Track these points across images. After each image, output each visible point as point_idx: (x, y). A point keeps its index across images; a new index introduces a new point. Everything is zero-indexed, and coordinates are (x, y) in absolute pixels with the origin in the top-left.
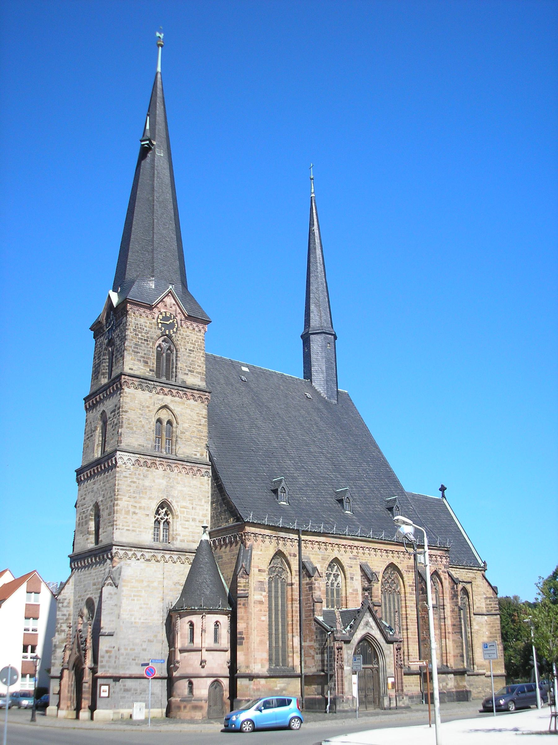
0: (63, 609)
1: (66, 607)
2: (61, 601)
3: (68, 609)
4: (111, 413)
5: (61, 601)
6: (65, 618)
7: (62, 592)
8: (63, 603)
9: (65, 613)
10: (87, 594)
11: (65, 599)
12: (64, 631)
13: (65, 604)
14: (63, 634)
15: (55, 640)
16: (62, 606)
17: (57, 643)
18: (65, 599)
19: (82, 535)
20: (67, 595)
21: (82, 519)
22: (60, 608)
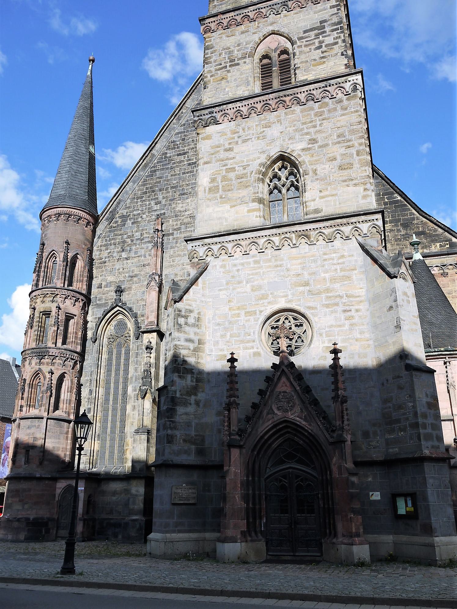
0: (187, 329)
1: (194, 325)
2: (183, 313)
3: (196, 329)
4: (305, 32)
5: (183, 313)
6: (191, 346)
7: (185, 298)
8: (186, 317)
9: (192, 336)
10: (276, 302)
11: (191, 311)
13: (191, 320)
14: (189, 377)
16: (186, 324)
17: (178, 395)
18: (191, 311)
19: (227, 207)
21: (224, 178)
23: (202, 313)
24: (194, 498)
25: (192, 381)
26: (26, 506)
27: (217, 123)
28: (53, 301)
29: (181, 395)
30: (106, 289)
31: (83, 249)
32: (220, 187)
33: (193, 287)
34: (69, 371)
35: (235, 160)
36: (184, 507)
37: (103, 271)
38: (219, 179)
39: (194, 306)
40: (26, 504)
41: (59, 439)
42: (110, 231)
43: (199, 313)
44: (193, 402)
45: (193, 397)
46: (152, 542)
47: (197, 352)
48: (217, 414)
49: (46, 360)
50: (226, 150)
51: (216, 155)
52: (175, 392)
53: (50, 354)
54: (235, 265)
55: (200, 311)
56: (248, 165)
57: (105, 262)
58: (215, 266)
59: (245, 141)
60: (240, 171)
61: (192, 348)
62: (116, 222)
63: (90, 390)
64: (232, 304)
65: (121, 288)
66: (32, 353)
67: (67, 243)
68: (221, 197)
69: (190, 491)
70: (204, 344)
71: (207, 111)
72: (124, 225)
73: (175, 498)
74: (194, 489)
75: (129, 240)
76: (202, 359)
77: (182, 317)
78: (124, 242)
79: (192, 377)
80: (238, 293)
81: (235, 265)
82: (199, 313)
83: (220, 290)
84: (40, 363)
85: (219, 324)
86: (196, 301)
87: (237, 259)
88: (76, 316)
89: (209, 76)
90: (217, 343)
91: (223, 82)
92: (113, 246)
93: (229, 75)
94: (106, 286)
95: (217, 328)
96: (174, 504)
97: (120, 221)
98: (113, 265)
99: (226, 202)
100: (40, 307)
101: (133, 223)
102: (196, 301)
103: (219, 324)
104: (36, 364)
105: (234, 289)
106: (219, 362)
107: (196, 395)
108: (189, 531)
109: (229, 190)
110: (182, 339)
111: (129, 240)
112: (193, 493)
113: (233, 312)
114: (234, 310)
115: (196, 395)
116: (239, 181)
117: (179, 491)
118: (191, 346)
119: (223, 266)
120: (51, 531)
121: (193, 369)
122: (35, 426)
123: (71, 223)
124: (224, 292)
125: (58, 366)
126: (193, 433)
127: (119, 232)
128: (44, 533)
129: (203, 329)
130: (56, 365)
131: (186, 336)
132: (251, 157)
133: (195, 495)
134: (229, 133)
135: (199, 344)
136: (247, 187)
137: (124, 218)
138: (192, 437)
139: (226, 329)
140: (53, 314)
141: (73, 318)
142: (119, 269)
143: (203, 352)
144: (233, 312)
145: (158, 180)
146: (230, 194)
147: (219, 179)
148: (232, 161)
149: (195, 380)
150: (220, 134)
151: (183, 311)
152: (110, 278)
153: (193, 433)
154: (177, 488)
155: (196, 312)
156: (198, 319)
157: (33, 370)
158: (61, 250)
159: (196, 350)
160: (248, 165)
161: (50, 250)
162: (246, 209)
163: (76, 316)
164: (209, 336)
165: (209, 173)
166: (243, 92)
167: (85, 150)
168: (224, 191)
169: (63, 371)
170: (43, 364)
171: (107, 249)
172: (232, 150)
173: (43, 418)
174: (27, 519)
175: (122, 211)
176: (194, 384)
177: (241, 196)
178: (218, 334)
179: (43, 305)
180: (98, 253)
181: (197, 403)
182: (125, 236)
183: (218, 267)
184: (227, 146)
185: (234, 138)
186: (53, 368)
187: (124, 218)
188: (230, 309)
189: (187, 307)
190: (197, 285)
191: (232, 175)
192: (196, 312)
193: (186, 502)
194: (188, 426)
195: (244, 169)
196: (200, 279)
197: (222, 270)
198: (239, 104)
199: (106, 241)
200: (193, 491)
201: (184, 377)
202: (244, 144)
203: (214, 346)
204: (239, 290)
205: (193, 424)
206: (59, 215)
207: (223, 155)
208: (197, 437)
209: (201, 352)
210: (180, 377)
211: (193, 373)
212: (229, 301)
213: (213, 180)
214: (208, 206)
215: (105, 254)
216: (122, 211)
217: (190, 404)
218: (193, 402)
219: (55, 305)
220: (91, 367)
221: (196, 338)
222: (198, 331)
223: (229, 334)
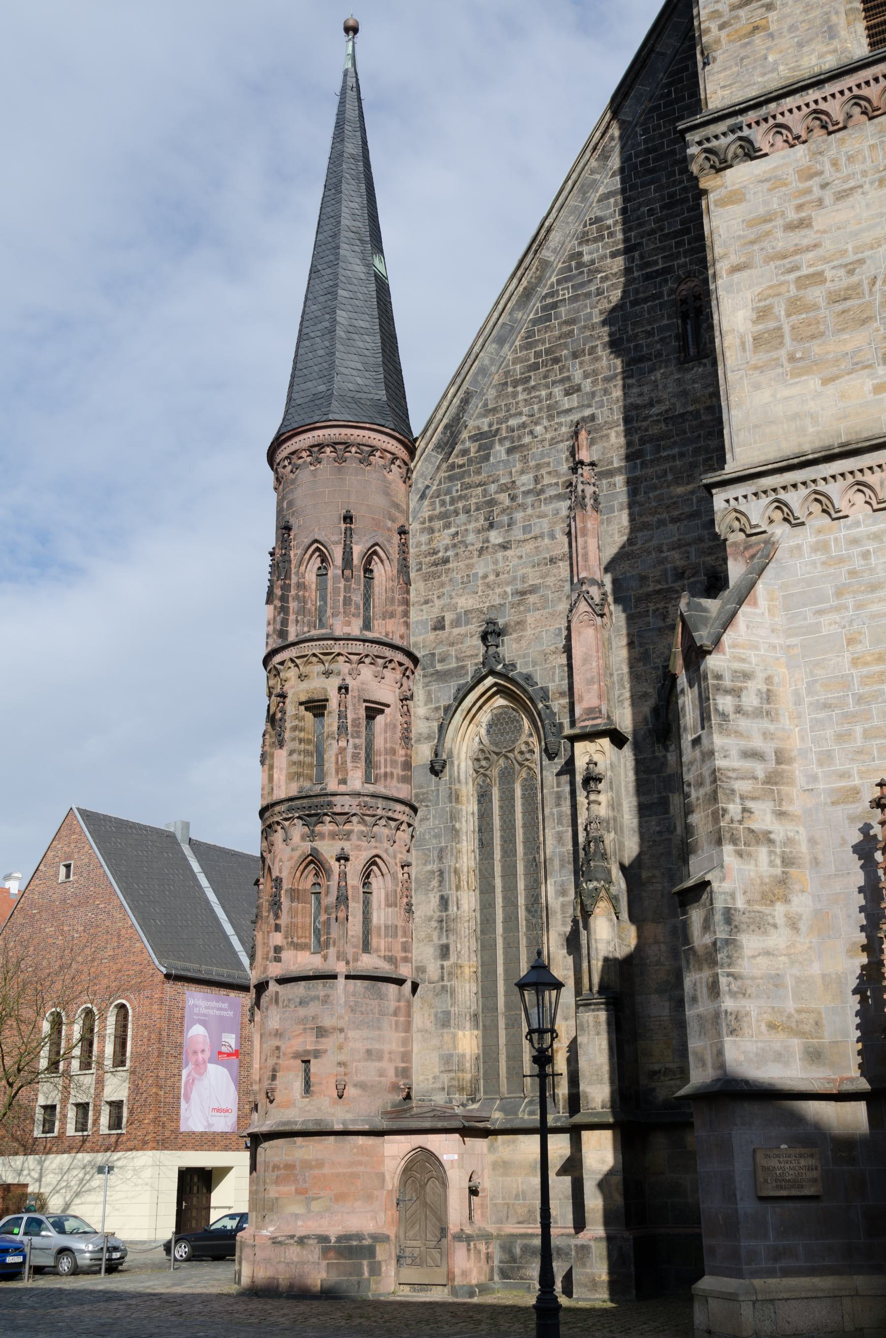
0: (743, 723)
1: (758, 713)
3: (765, 724)
5: (727, 683)
8: (736, 692)
9: (757, 743)
11: (747, 676)
12: (766, 838)
13: (750, 700)
14: (762, 852)
15: (726, 886)
16: (739, 710)
17: (740, 904)
18: (747, 676)
19: (813, 383)
20: (753, 657)
21: (795, 306)
22: (724, 716)
23: (776, 680)
24: (815, 1181)
25: (771, 864)
26: (315, 1206)
27: (751, 152)
28: (328, 674)
29: (748, 902)
30: (456, 631)
31: (389, 530)
32: (787, 329)
33: (744, 608)
34: (386, 851)
35: (820, 252)
36: (790, 1205)
37: (442, 585)
38: (780, 310)
39: (754, 660)
40: (314, 1199)
41: (379, 1028)
42: (451, 478)
43: (769, 680)
44: (780, 920)
45: (780, 909)
46: (710, 1300)
47: (776, 784)
48: (848, 951)
49: (327, 827)
50: (791, 227)
51: (765, 244)
52: (733, 895)
53: (338, 809)
54: (855, 542)
55: (769, 672)
56: (861, 262)
57: (446, 561)
58: (799, 547)
59: (842, 196)
60: (836, 279)
61: (761, 775)
62: (465, 452)
63: (442, 897)
64: (859, 648)
65: (495, 624)
66: (290, 810)
67: (348, 518)
68: (792, 359)
69: (803, 1162)
70: (790, 761)
71: (722, 127)
72: (487, 458)
73: (766, 1181)
74: (812, 1156)
75: (504, 498)
76: (791, 801)
77: (727, 692)
78: (492, 503)
79: (771, 853)
80: (873, 617)
81: (855, 542)
82: (769, 680)
83: (820, 612)
84: (312, 836)
85: (826, 706)
86: (757, 648)
87: (857, 524)
88: (388, 706)
89: (714, 26)
90: (826, 758)
91: (758, 38)
92: (463, 517)
93: (772, 16)
94: (457, 623)
95: (822, 715)
96: (762, 1199)
97: (473, 447)
98: (470, 567)
99: (807, 371)
100: (297, 690)
101: (509, 451)
102: (757, 648)
103: (826, 706)
104: (303, 838)
105: (859, 606)
106: (839, 808)
107: (787, 901)
108: (813, 1272)
109: (813, 337)
110: (734, 753)
111: (504, 498)
112: (810, 1168)
113: (865, 671)
114: (866, 664)
115: (787, 901)
116: (839, 307)
117: (774, 1163)
118: (760, 769)
119: (822, 547)
120: (384, 1269)
121: (770, 832)
122: (317, 998)
123: (352, 465)
124: (836, 617)
125: (359, 839)
126: (791, 1006)
127: (476, 479)
128: (366, 1274)
129: (785, 721)
130: (354, 837)
131: (744, 744)
132: (867, 238)
133: (815, 1174)
134: (792, 178)
135: (779, 762)
136: (864, 322)
137: (485, 439)
138: (789, 1016)
139: (850, 718)
140: (333, 704)
141: (382, 712)
142: (485, 576)
143: (791, 782)
144: (865, 671)
145: (566, 329)
146: (816, 348)
147: (780, 310)
148: (810, 255)
149: (778, 861)
150: (766, 186)
151: (727, 676)
152: (465, 602)
153: (791, 1006)
154: (767, 1156)
155: (761, 676)
156: (768, 696)
157: (297, 853)
158: (335, 538)
159: (772, 779)
160: (861, 262)
161: (307, 541)
162: (869, 384)
163: (388, 706)
164: (802, 739)
165: (749, 295)
166: (818, 59)
167: (364, 269)
168: (798, 339)
169: (375, 852)
170: (322, 836)
171: (447, 526)
172: (809, 225)
173: (335, 977)
174: (323, 1239)
175: (476, 422)
176: (778, 871)
177: (849, 348)
178: (829, 733)
179: (304, 685)
180: (424, 538)
181: (793, 924)
182: (493, 488)
183: (806, 549)
184: (792, 216)
185: (809, 191)
186: (347, 845)
187: (485, 439)
188: (855, 662)
189: (737, 666)
190: (755, 604)
191: (816, 294)
192: (761, 676)
193: (794, 1192)
194: (776, 986)
195: (851, 272)
196: (760, 587)
197: (819, 557)
198: (813, 95)
199: (443, 503)
200: (811, 1162)
201: (750, 855)
202: (841, 205)
203: (821, 764)
204: (875, 608)
205: (789, 981)
206: (321, 446)
207: (782, 241)
208: (804, 1015)
209: (787, 784)
210: (740, 854)
211: (771, 841)
212: (851, 641)
213: (763, 314)
214: (757, 387)
215: (444, 539)
216: (476, 422)
217: (775, 926)
218: (780, 920)
219: (335, 682)
220: (437, 836)
221: (768, 748)
222: (772, 728)
223: (858, 729)
